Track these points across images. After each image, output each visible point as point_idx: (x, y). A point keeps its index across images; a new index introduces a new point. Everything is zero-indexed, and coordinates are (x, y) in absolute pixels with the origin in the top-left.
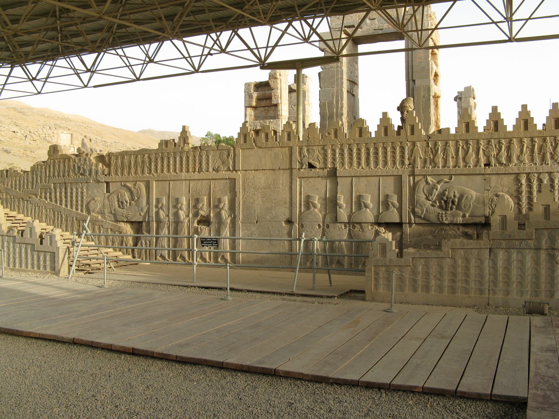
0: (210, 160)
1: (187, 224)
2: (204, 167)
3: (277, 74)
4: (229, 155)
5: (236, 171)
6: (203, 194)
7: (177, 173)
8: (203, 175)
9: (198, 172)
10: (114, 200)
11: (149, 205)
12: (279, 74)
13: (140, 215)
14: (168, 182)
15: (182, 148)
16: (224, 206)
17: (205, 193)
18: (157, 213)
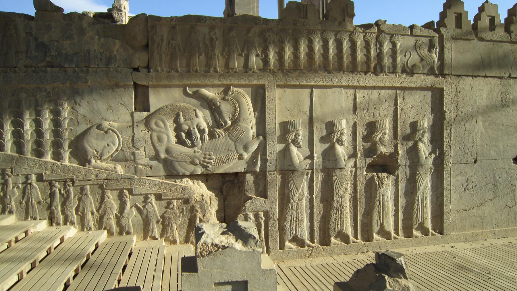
1: (351, 172)
6: (381, 114)
10: (166, 129)
11: (265, 138)
13: (241, 157)
17: (385, 112)
18: (286, 153)
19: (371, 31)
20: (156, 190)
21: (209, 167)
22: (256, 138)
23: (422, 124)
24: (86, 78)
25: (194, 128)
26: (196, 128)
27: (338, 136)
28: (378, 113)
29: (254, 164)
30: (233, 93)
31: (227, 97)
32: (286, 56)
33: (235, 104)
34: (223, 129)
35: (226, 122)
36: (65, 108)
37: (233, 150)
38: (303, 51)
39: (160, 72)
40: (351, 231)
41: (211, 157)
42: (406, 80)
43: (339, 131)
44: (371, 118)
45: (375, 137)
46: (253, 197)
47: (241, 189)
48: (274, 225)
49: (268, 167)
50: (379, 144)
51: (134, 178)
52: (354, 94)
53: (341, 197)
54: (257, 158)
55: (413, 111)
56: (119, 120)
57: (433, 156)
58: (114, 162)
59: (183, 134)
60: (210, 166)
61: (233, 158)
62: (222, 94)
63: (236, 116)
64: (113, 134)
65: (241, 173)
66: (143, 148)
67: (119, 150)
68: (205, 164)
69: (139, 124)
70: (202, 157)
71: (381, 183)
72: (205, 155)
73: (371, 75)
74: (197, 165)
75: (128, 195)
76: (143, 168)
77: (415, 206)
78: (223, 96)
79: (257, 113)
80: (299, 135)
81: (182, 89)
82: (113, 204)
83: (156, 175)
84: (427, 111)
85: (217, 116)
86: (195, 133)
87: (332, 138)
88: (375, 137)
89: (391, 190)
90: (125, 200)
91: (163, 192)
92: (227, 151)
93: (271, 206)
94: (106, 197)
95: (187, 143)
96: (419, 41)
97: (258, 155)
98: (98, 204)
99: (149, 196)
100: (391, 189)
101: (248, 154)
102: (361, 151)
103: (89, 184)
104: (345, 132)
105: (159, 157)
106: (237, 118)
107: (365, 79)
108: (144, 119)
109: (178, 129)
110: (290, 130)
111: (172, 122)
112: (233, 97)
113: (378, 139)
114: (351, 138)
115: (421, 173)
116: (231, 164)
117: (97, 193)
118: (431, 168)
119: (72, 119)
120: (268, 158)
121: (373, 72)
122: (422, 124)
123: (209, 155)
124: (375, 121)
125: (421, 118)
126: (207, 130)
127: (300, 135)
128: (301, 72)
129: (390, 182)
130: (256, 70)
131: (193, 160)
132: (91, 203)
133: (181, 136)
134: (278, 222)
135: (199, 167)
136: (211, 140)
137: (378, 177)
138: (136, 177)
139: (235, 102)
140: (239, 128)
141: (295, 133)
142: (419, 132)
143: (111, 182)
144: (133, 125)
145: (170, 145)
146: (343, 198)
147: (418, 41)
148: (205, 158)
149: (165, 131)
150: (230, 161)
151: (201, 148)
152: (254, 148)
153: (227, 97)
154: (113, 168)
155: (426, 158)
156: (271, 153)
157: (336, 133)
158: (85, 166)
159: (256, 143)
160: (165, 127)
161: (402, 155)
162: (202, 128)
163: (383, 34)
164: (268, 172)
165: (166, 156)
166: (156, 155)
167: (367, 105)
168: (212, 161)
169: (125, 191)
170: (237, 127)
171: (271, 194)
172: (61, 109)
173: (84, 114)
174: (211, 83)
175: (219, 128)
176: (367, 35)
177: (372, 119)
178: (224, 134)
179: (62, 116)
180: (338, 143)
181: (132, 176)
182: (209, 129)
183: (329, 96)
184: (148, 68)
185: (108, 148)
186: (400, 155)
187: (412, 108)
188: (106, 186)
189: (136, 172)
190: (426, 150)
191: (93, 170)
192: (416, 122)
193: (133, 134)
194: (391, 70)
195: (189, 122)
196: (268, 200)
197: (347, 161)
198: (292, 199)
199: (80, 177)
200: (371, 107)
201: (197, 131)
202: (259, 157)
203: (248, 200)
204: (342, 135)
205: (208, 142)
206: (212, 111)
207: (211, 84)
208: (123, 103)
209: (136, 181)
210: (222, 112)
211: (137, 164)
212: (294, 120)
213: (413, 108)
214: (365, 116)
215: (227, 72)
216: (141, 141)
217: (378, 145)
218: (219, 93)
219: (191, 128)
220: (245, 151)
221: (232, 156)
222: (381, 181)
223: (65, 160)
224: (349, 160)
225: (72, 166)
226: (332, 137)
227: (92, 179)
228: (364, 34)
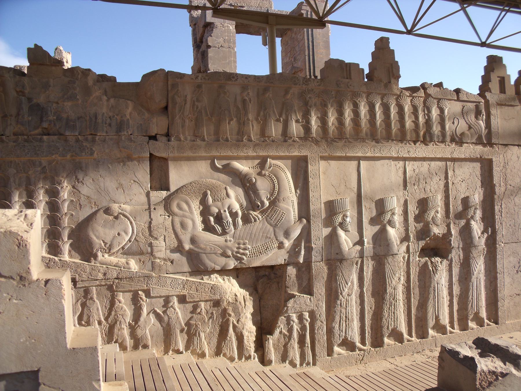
1: (404, 258)
6: (432, 189)
10: (191, 212)
11: (309, 221)
13: (281, 246)
19: (419, 95)
20: (179, 291)
21: (244, 259)
22: (299, 222)
24: (91, 149)
25: (225, 211)
26: (227, 210)
29: (297, 254)
30: (271, 166)
31: (263, 172)
33: (273, 181)
34: (259, 212)
35: (262, 203)
36: (65, 187)
37: (272, 237)
39: (183, 141)
40: (405, 328)
41: (246, 246)
43: (390, 211)
44: (422, 194)
45: (428, 217)
46: (296, 295)
47: (280, 285)
48: (322, 328)
49: (313, 257)
50: (432, 225)
51: (152, 277)
52: (403, 167)
53: (394, 289)
54: (301, 245)
55: (464, 185)
56: (132, 201)
57: (486, 235)
58: (125, 256)
59: (212, 219)
60: (245, 257)
61: (272, 247)
62: (257, 168)
63: (275, 194)
64: (125, 219)
65: (281, 265)
66: (163, 237)
67: (133, 240)
68: (239, 255)
69: (156, 207)
70: (235, 247)
72: (239, 244)
73: (420, 145)
74: (229, 257)
75: (144, 297)
76: (162, 263)
77: (470, 294)
78: (259, 170)
79: (298, 191)
80: (347, 217)
81: (209, 161)
82: (125, 310)
83: (179, 271)
84: (477, 185)
85: (252, 195)
86: (227, 217)
87: (383, 219)
88: (428, 217)
89: (445, 277)
90: (141, 304)
91: (188, 293)
92: (265, 238)
93: (317, 305)
94: (117, 301)
95: (216, 230)
96: (465, 106)
97: (301, 243)
98: (106, 310)
99: (171, 298)
100: (445, 276)
101: (289, 241)
102: (413, 233)
103: (95, 285)
104: (396, 212)
105: (183, 248)
106: (276, 198)
107: (414, 148)
108: (163, 200)
109: (205, 212)
110: (337, 211)
111: (198, 203)
112: (271, 172)
113: (430, 219)
114: (402, 219)
115: (475, 255)
116: (270, 255)
117: (105, 296)
118: (484, 249)
119: (73, 201)
120: (313, 245)
121: (422, 141)
123: (244, 244)
125: (472, 193)
126: (240, 213)
127: (348, 216)
128: (347, 141)
129: (444, 268)
131: (225, 251)
132: (98, 309)
133: (210, 221)
134: (325, 323)
135: (232, 260)
136: (245, 225)
137: (432, 262)
138: (154, 275)
139: (273, 178)
140: (278, 210)
141: (342, 215)
143: (122, 282)
144: (149, 208)
145: (195, 233)
148: (239, 248)
149: (190, 215)
150: (269, 250)
151: (234, 235)
152: (296, 233)
153: (263, 172)
154: (126, 264)
155: (479, 238)
156: (316, 240)
157: (387, 213)
158: (90, 262)
159: (299, 227)
160: (189, 209)
161: (455, 235)
162: (234, 211)
163: (430, 99)
164: (313, 263)
165: (191, 247)
166: (178, 246)
167: (417, 180)
168: (247, 252)
169: (140, 292)
170: (277, 209)
171: (318, 290)
172: (60, 188)
173: (88, 195)
174: (244, 154)
175: (254, 211)
176: (414, 100)
177: (423, 196)
178: (260, 217)
179: (60, 197)
180: (390, 225)
181: (149, 274)
182: (242, 211)
183: (378, 169)
184: (168, 135)
185: (119, 237)
186: (453, 237)
188: (117, 287)
189: (153, 268)
191: (100, 267)
193: (150, 220)
194: (441, 138)
195: (219, 204)
196: (314, 298)
197: (400, 246)
198: (341, 294)
199: (84, 276)
201: (228, 215)
202: (303, 244)
203: (291, 298)
205: (241, 229)
206: (246, 188)
207: (244, 156)
208: (136, 180)
209: (154, 280)
210: (258, 190)
211: (155, 258)
212: (341, 199)
213: (464, 181)
215: (264, 141)
216: (160, 228)
218: (253, 167)
219: (222, 211)
220: (286, 238)
221: (270, 244)
222: (435, 267)
223: (64, 254)
225: (74, 262)
226: (383, 218)
227: (99, 279)
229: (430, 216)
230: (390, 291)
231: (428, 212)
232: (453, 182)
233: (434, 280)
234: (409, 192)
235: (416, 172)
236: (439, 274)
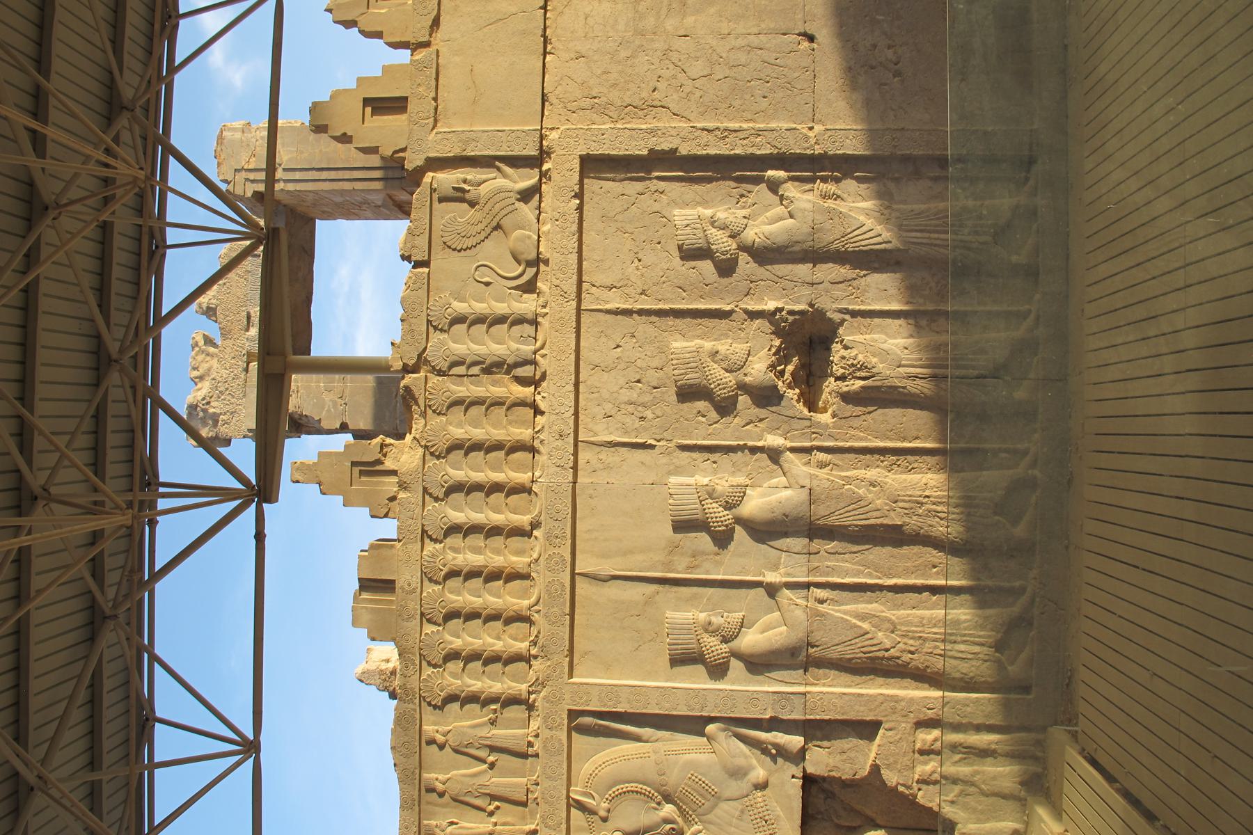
0: (480, 308)
1: (822, 465)
2: (514, 346)
3: (384, 668)
4: (459, 196)
5: (544, 154)
6: (656, 363)
7: (535, 525)
8: (555, 362)
9: (535, 382)
11: (712, 720)
12: (383, 663)
14: (582, 586)
15: (403, 486)
16: (724, 227)
18: (759, 664)
22: (712, 742)
23: (688, 230)
27: (714, 505)
28: (652, 372)
32: (493, 645)
38: (480, 597)
42: (557, 282)
43: (703, 505)
48: (959, 707)
50: (745, 375)
52: (598, 449)
57: (790, 190)
71: (859, 370)
84: (650, 210)
89: (886, 334)
100: (883, 336)
107: (554, 417)
113: (730, 379)
118: (825, 196)
122: (688, 230)
124: (676, 386)
130: (531, 729)
137: (842, 378)
142: (711, 240)
146: (899, 495)
147: (445, 243)
155: (791, 217)
167: (631, 408)
171: (870, 710)
186: (780, 305)
187: (640, 260)
190: (768, 214)
192: (680, 248)
194: (528, 329)
197: (792, 481)
198: (887, 650)
200: (636, 396)
204: (715, 495)
214: (660, 414)
217: (748, 379)
224: (788, 474)
226: (720, 526)
228: (429, 412)
229: (724, 380)
230: (899, 515)
231: (712, 386)
232: (641, 294)
233: (887, 378)
234: (662, 437)
235: (613, 413)
236: (874, 360)
